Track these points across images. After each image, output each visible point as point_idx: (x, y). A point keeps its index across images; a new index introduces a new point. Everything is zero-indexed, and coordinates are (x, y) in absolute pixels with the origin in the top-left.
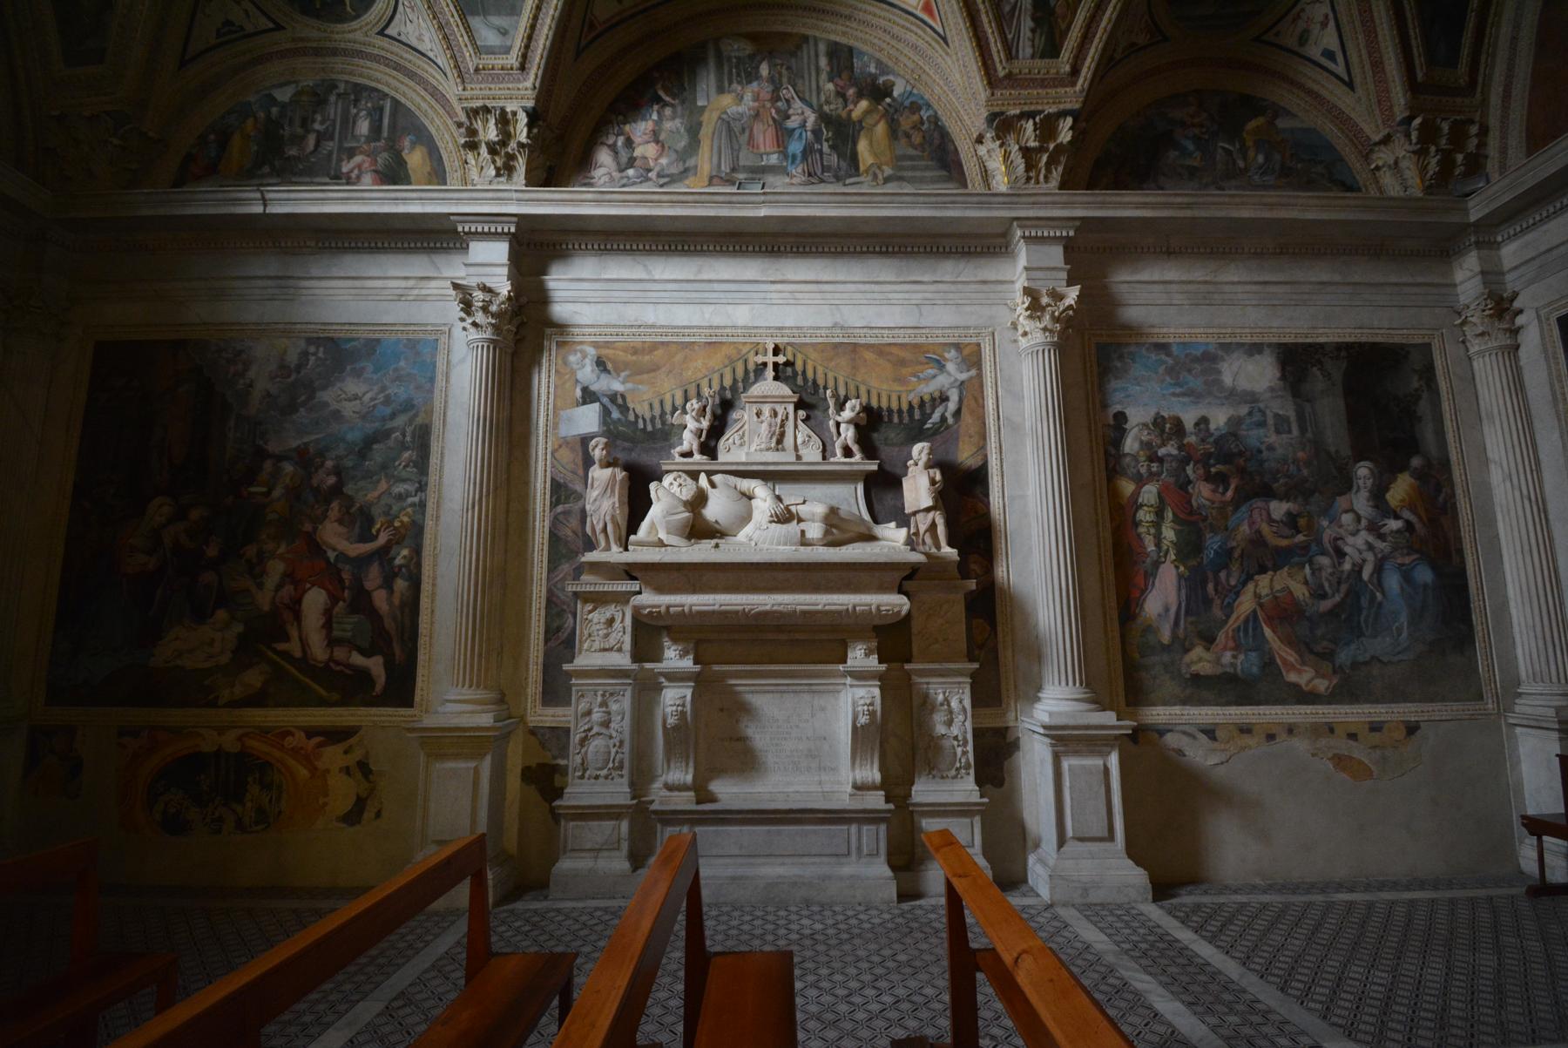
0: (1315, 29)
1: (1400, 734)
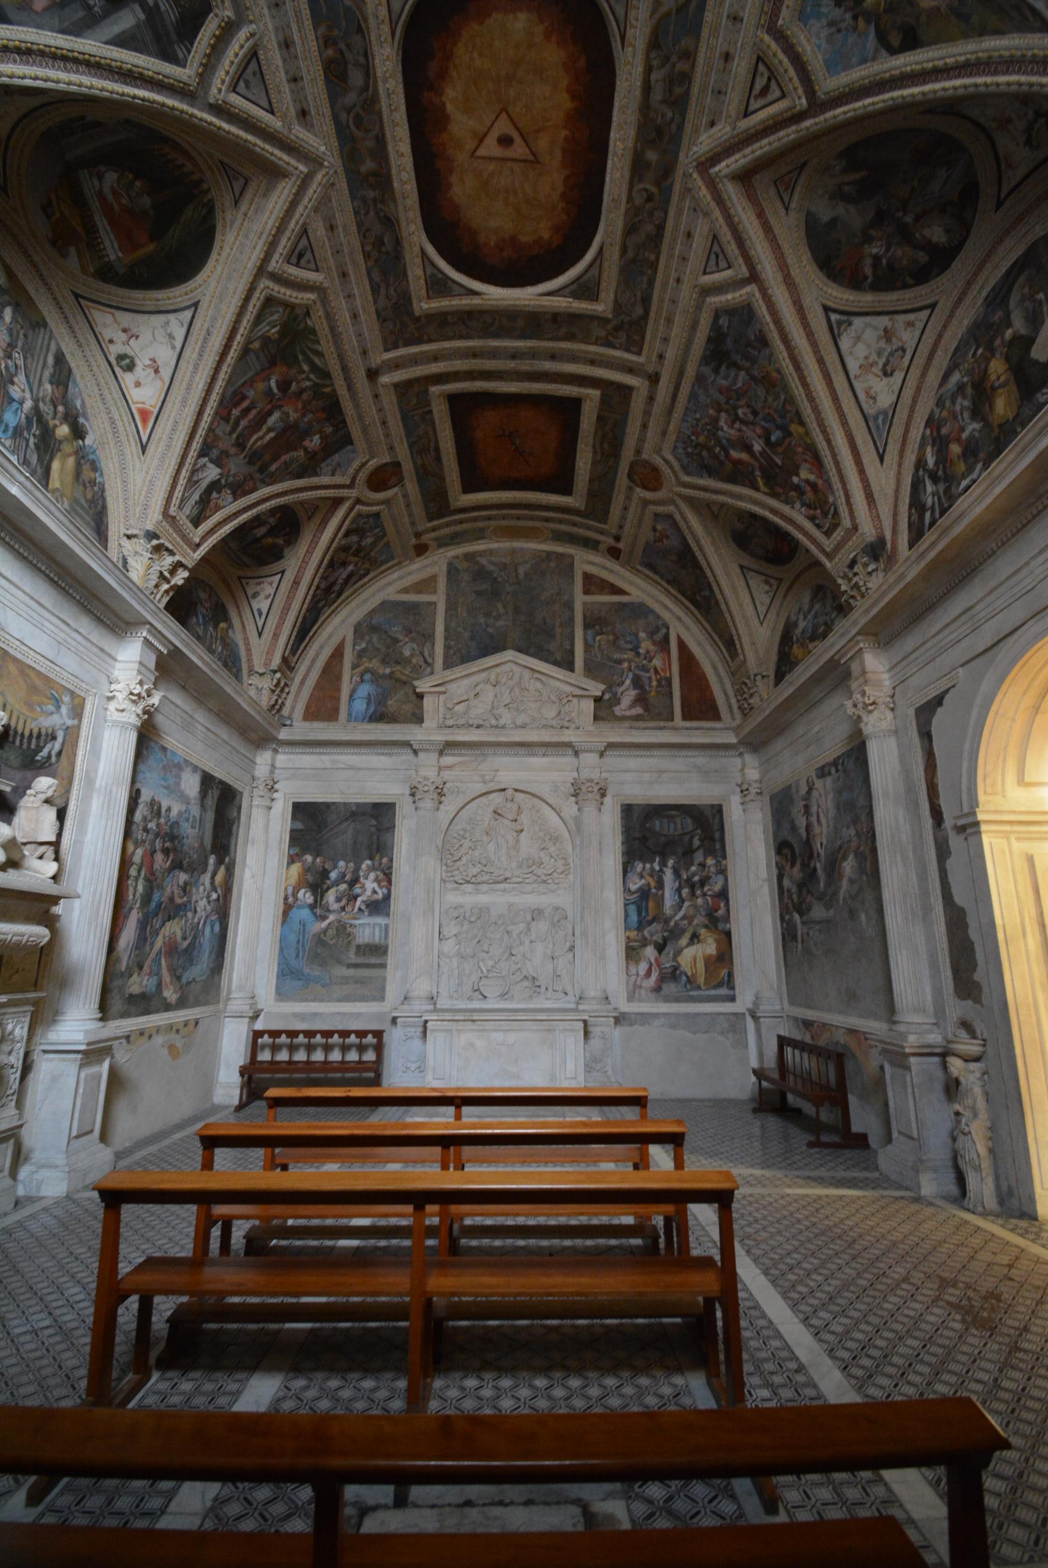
0: (262, 596)
1: (191, 1026)
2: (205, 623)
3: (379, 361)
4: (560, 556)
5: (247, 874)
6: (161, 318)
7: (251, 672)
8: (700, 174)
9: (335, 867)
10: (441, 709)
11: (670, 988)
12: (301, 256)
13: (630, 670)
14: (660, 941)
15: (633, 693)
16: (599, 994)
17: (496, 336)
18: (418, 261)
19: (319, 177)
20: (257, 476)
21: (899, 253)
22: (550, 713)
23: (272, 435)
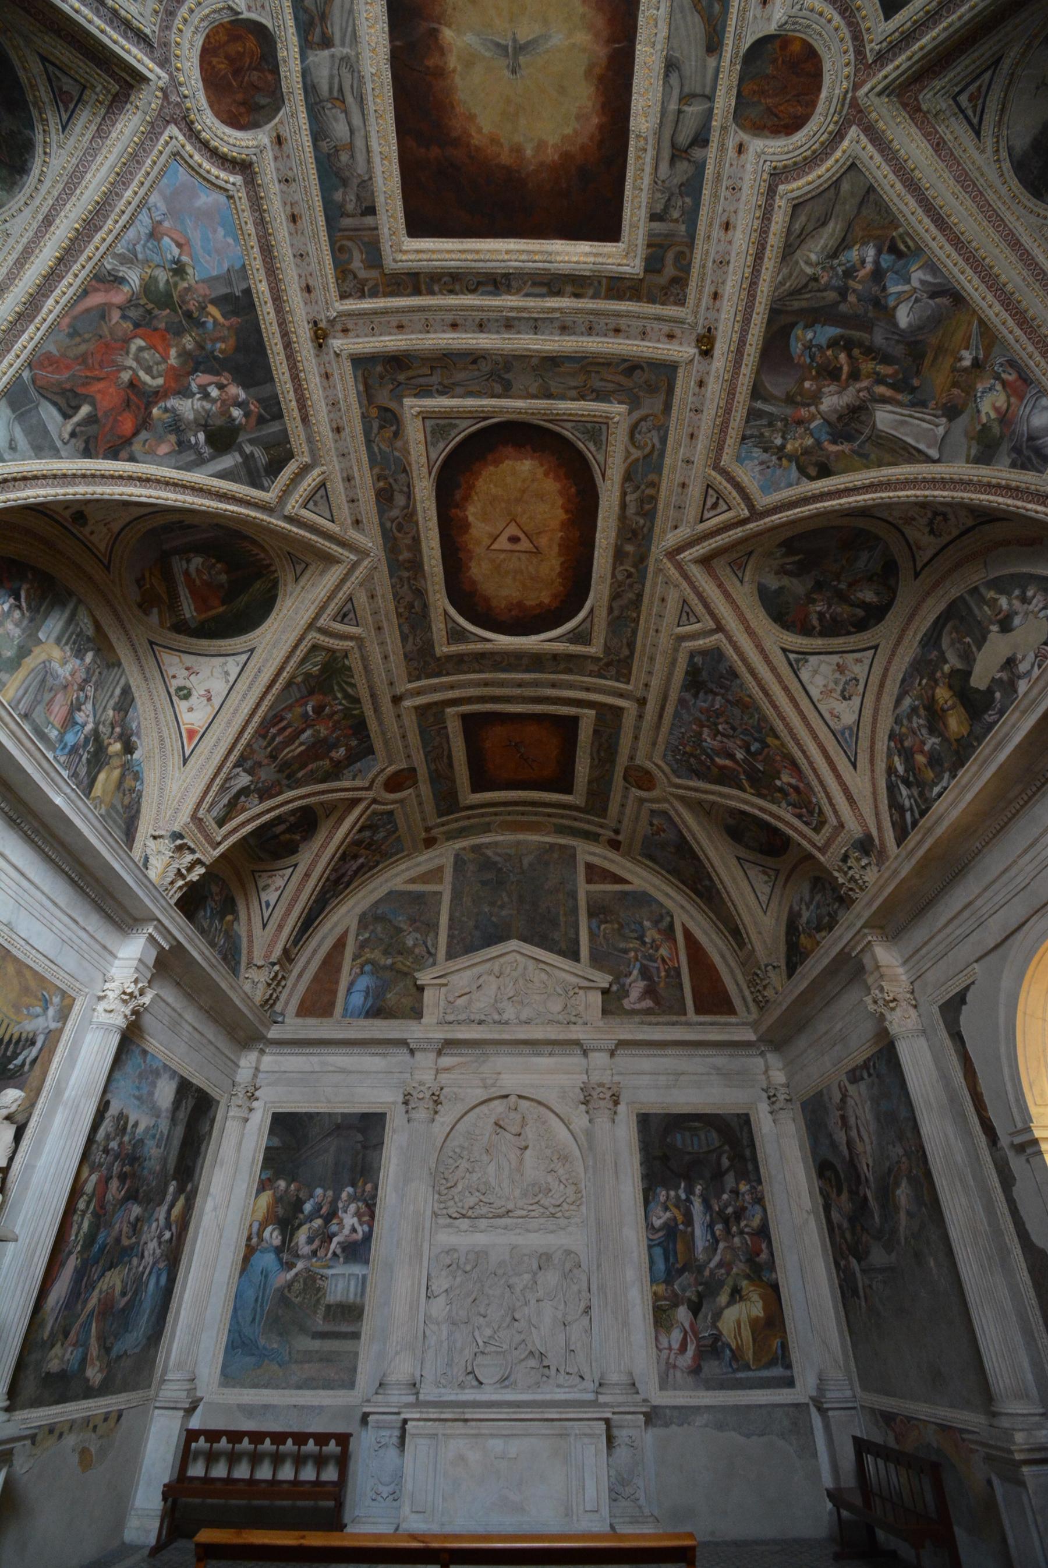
0: (273, 888)
2: (212, 918)
3: (403, 690)
4: (562, 847)
5: (209, 1205)
6: (221, 659)
7: (250, 964)
8: (669, 559)
9: (311, 1196)
10: (442, 1003)
11: (712, 1368)
12: (345, 615)
13: (637, 959)
14: (694, 1298)
15: (641, 984)
16: (624, 1379)
17: (504, 670)
18: (442, 618)
19: (366, 563)
20: (285, 782)
21: (839, 610)
22: (555, 1006)
23: (303, 748)
